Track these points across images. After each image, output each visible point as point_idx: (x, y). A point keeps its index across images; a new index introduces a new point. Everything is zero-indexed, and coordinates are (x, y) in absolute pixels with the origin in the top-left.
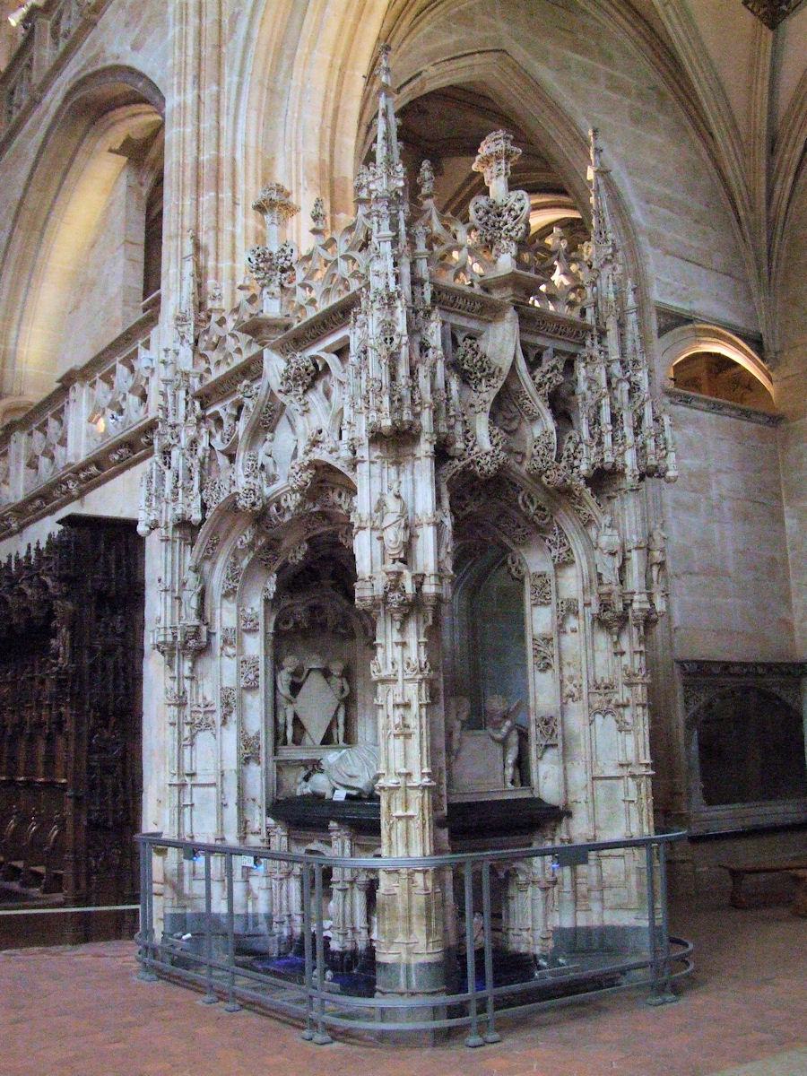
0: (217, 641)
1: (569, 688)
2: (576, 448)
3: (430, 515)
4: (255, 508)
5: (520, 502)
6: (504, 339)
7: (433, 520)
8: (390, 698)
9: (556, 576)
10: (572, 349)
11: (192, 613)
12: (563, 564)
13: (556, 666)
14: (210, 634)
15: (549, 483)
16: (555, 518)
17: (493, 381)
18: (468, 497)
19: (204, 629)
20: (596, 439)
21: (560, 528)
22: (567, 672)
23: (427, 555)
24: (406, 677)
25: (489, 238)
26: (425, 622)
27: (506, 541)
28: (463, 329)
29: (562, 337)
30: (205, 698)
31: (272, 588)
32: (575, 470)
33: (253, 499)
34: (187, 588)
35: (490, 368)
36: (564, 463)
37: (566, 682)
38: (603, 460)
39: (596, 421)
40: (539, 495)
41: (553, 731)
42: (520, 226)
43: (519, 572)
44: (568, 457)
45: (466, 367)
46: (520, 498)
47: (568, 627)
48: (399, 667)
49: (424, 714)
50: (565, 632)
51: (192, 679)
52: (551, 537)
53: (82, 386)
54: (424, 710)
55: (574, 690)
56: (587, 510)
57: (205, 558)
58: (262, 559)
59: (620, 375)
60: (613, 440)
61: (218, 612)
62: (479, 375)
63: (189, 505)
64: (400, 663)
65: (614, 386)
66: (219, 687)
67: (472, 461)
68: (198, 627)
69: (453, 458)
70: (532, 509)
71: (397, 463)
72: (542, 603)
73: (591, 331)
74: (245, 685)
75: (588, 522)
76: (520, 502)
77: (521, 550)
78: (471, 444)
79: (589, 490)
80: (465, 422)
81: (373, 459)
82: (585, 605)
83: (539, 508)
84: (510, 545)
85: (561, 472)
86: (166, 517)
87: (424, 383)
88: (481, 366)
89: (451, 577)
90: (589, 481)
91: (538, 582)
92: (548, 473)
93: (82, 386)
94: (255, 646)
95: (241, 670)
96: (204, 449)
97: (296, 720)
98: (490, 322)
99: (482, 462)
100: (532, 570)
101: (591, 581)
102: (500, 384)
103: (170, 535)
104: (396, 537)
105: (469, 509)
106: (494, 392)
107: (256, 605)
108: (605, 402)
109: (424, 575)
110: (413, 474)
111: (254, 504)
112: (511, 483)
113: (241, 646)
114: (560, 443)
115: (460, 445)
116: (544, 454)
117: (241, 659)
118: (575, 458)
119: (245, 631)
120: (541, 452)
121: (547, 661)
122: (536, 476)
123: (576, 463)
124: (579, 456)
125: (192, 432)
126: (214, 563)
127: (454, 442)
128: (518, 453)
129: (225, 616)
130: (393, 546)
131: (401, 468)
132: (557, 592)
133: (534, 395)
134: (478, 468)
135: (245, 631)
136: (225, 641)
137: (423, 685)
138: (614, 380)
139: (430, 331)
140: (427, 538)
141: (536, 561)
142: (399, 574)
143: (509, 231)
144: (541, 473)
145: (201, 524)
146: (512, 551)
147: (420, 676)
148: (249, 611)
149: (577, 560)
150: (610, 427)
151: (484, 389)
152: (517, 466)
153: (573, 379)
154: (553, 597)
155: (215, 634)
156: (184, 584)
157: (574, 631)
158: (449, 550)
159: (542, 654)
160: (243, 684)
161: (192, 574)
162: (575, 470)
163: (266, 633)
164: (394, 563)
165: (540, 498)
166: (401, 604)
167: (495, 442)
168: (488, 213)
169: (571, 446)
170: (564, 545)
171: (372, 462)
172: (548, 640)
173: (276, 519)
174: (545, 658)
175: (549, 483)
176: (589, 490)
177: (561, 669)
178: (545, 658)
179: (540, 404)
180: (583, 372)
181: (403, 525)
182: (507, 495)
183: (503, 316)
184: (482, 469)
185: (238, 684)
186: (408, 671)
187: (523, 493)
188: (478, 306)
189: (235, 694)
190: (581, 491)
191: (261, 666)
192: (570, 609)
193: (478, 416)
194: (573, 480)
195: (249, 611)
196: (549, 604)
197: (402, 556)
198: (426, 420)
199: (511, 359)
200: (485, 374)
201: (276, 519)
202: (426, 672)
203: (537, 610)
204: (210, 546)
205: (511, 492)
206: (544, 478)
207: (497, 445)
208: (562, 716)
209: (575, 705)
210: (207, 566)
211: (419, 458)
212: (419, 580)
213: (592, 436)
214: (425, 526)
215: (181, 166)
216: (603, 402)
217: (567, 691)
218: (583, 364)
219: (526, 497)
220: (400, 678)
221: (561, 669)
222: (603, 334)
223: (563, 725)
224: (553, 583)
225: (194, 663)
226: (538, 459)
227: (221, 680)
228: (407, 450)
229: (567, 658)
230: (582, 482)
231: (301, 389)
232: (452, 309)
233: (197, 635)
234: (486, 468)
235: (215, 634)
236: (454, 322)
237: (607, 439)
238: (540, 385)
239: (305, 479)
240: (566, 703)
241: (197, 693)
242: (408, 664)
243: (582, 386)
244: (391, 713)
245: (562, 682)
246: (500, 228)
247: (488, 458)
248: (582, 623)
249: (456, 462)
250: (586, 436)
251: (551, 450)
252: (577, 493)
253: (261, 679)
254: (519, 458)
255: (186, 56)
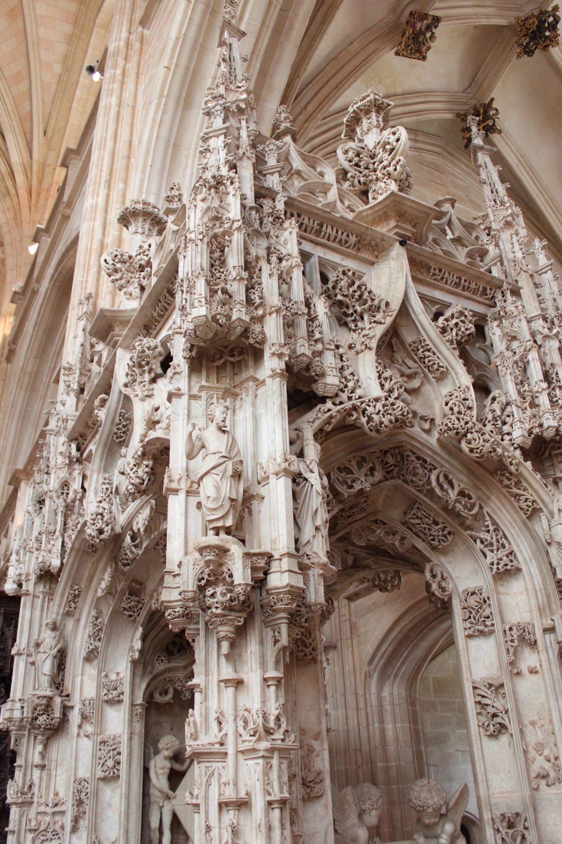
0: (75, 717)
1: (539, 764)
2: (503, 410)
3: (279, 460)
4: (102, 536)
5: (434, 483)
6: (390, 278)
7: (285, 465)
8: (214, 791)
9: (498, 593)
10: (480, 309)
11: (45, 681)
12: (506, 573)
13: (513, 727)
14: (66, 709)
15: (471, 450)
16: (486, 509)
17: (379, 316)
18: (355, 469)
19: (58, 700)
20: (528, 399)
21: (494, 523)
22: (533, 736)
23: (274, 527)
24: (243, 747)
25: (362, 179)
26: (276, 642)
27: (421, 545)
28: (335, 266)
29: (466, 293)
30: (56, 794)
31: (138, 645)
32: (507, 438)
33: (100, 524)
34: (41, 649)
35: (373, 300)
36: (489, 427)
37: (532, 754)
38: (541, 425)
39: (523, 380)
40: (461, 476)
41: (523, 838)
42: (397, 159)
43: (443, 589)
44: (495, 419)
45: (339, 297)
46: (433, 478)
47: (524, 667)
48: (229, 727)
49: (276, 824)
50: (519, 674)
51: (43, 767)
52: (483, 535)
53: (27, 484)
54: (276, 813)
55: (547, 766)
56: (529, 495)
57: (68, 614)
58: (125, 609)
59: (546, 331)
60: (551, 401)
61: (78, 680)
62: (359, 309)
63: (50, 552)
64: (231, 718)
65: (539, 343)
66: (72, 779)
67: (355, 408)
68: (50, 699)
69: (323, 400)
70: (453, 495)
71: (231, 394)
72: (481, 632)
73: (500, 287)
74: (102, 775)
75: (533, 513)
76: (434, 483)
77: (443, 559)
78: (351, 384)
79: (529, 464)
80: (341, 357)
81: (195, 391)
82: (545, 630)
83: (461, 493)
84: (428, 552)
85: (487, 437)
86: (29, 568)
87: (269, 286)
88: (361, 296)
89: (324, 566)
90: (527, 454)
91: (472, 601)
92: (469, 436)
93: (27, 484)
94: (117, 722)
95: (99, 754)
96: (75, 492)
97: (176, 822)
98: (372, 264)
99: (370, 410)
100: (461, 590)
101: (548, 596)
102: (389, 321)
103: (31, 589)
104: (218, 488)
105: (357, 487)
106: (379, 330)
107: (121, 667)
108: (533, 356)
109: (270, 557)
110: (254, 405)
111: (101, 531)
112: (418, 458)
113: (100, 723)
114: (482, 407)
115: (332, 380)
116: (459, 413)
117: (100, 738)
118: (504, 423)
119: (107, 702)
120: (456, 409)
121: (499, 720)
122: (452, 443)
123: (506, 428)
124: (509, 420)
125: (63, 474)
126: (78, 620)
127: (323, 375)
128: (423, 418)
129: (84, 683)
130: (213, 506)
131: (238, 403)
132: (501, 613)
133: (438, 341)
134: (364, 420)
135: (107, 702)
136: (84, 717)
137: (275, 762)
138: (539, 338)
139: (282, 239)
140: (276, 497)
141: (463, 574)
142: (223, 551)
143: (384, 168)
144: (461, 436)
145: (60, 570)
146: (429, 561)
147: (264, 745)
148: (113, 677)
149: (523, 567)
150: (545, 385)
151: (368, 326)
152: (424, 435)
153: (488, 343)
154: (497, 620)
155: (72, 707)
156: (38, 645)
157: (533, 671)
158: (319, 522)
159: (491, 710)
160: (100, 774)
161: (49, 632)
162: (507, 438)
163: (133, 705)
164: (217, 534)
165: (461, 481)
166: (229, 608)
167: (387, 386)
168: (358, 155)
169: (496, 406)
170: (503, 546)
171: (192, 397)
172: (497, 688)
173: (132, 552)
174: (495, 715)
175: (471, 450)
176: (529, 464)
177: (521, 731)
178: (495, 715)
179: (447, 353)
180: (498, 331)
181: (230, 472)
182: (415, 474)
183: (387, 255)
184: (370, 419)
185: (93, 774)
186: (246, 737)
187: (435, 472)
188: (353, 239)
189: (90, 788)
190: (517, 465)
191: (124, 749)
192: (524, 639)
193: (360, 355)
194: (504, 449)
195: (113, 677)
196: (491, 632)
197: (229, 522)
198: (273, 329)
199: (401, 296)
200: (366, 306)
201: (132, 552)
202: (279, 735)
203: (474, 643)
204: (71, 598)
205: (420, 471)
206: (464, 446)
207: (391, 391)
208: (535, 810)
209: (552, 791)
210: (70, 624)
211: (264, 382)
212: (260, 567)
213: (522, 396)
214: (273, 478)
215: (89, 251)
216: (530, 357)
217: (535, 769)
218: (495, 323)
219: (442, 479)
220: (231, 750)
221: (521, 731)
222: (516, 292)
223: (538, 829)
224: (493, 601)
225: (45, 746)
226: (453, 417)
227: (76, 768)
228: (245, 375)
229: (529, 715)
230: (518, 453)
231: (147, 377)
232: (319, 240)
233: (48, 707)
234: (375, 417)
235: (72, 707)
236: (322, 255)
237: (543, 400)
238: (444, 330)
239: (140, 473)
240: (537, 789)
241: (48, 786)
242: (246, 722)
243: (500, 346)
244: (214, 821)
245: (525, 752)
246: (375, 170)
247: (379, 406)
248: (543, 656)
249: (329, 404)
250: (513, 395)
251: (469, 408)
252: (512, 468)
253: (123, 767)
254: (427, 426)
255: (101, 171)
